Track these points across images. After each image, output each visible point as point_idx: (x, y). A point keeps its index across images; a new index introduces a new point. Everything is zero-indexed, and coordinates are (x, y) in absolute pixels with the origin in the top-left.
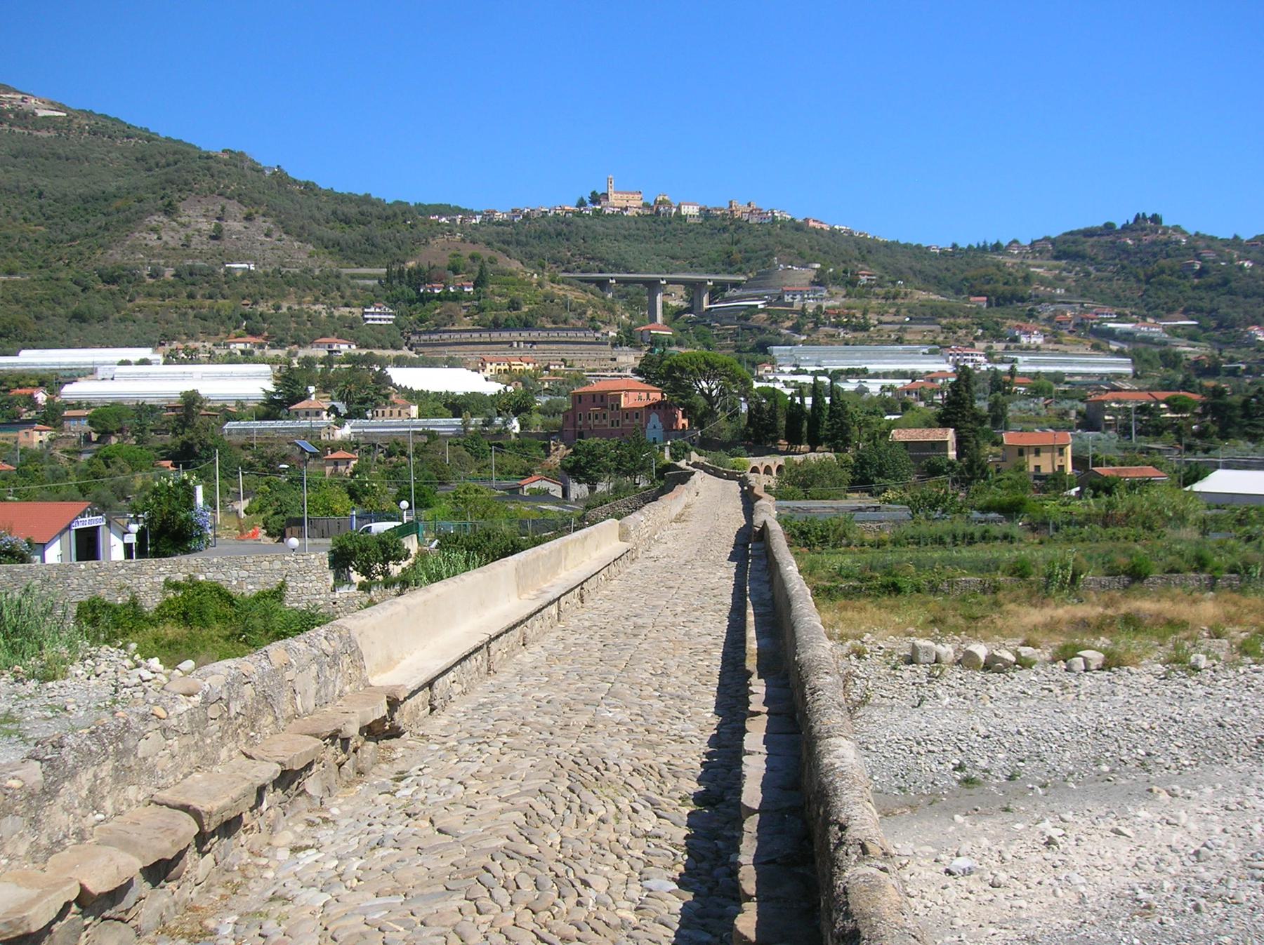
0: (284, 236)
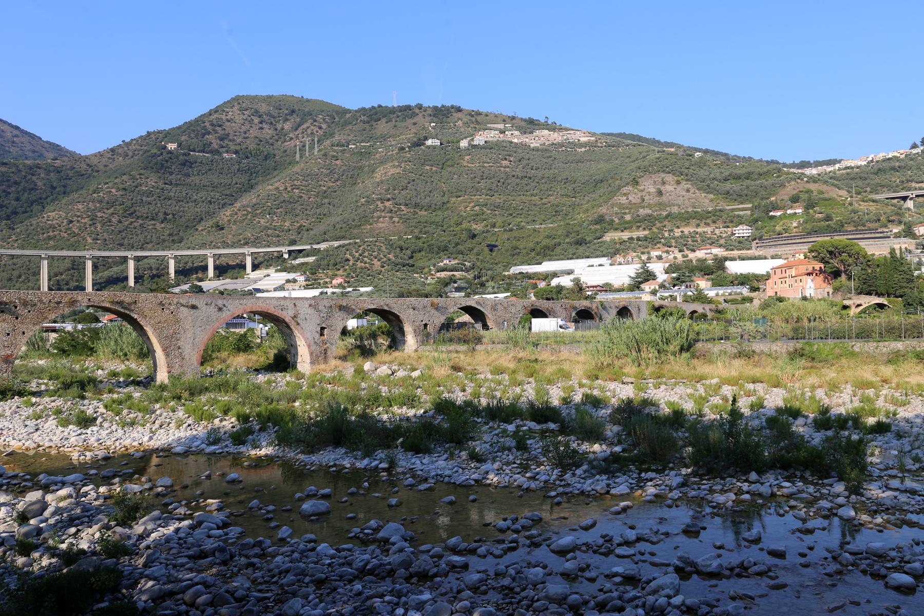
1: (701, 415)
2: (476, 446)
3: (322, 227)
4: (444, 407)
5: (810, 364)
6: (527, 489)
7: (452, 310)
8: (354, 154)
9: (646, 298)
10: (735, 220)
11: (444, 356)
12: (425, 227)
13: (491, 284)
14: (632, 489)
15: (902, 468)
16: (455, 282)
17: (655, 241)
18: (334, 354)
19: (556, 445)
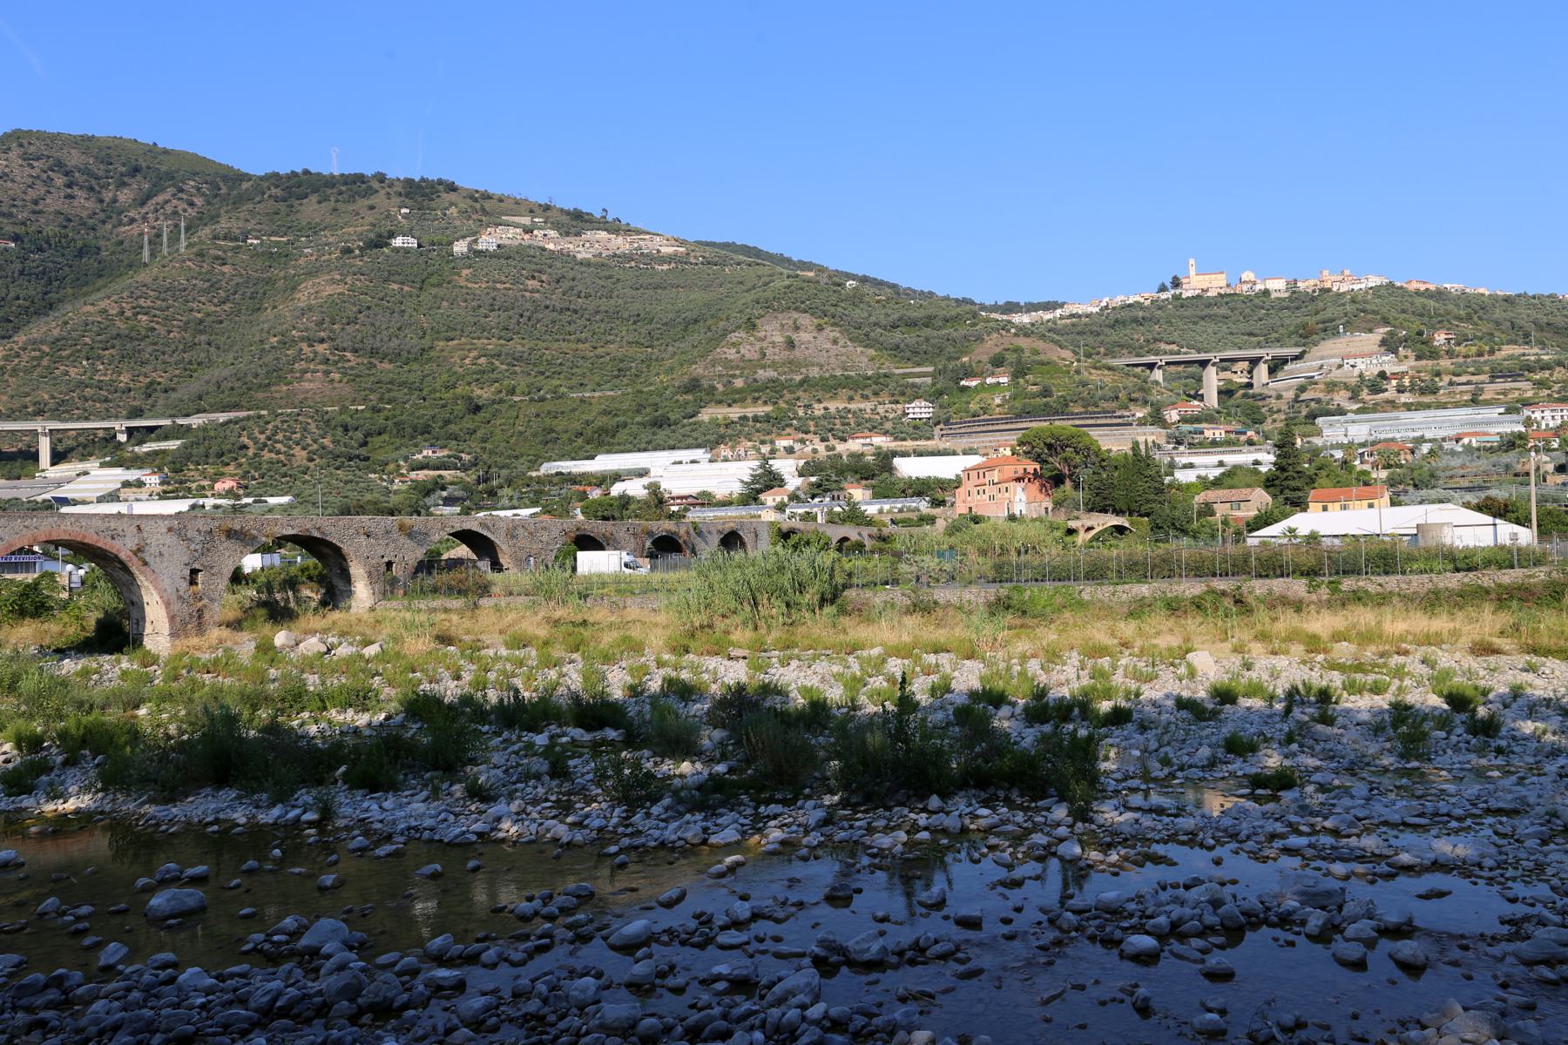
1: (855, 708)
2: (480, 773)
3: (195, 386)
4: (421, 707)
5: (1018, 622)
6: (568, 843)
7: (437, 538)
8: (257, 255)
9: (769, 516)
10: (909, 391)
11: (423, 617)
12: (389, 391)
13: (507, 491)
14: (743, 833)
15: (1146, 777)
16: (443, 489)
17: (783, 423)
18: (216, 618)
19: (618, 766)
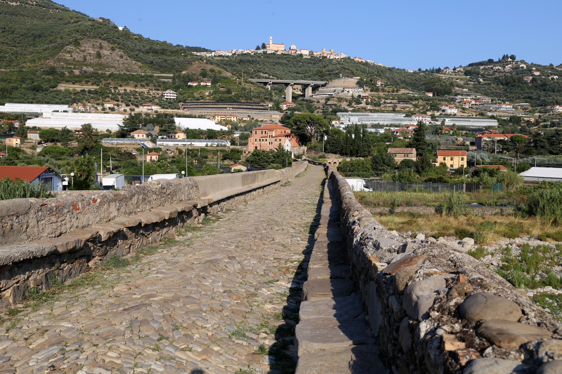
0: (128, 58)
17: (105, 95)
